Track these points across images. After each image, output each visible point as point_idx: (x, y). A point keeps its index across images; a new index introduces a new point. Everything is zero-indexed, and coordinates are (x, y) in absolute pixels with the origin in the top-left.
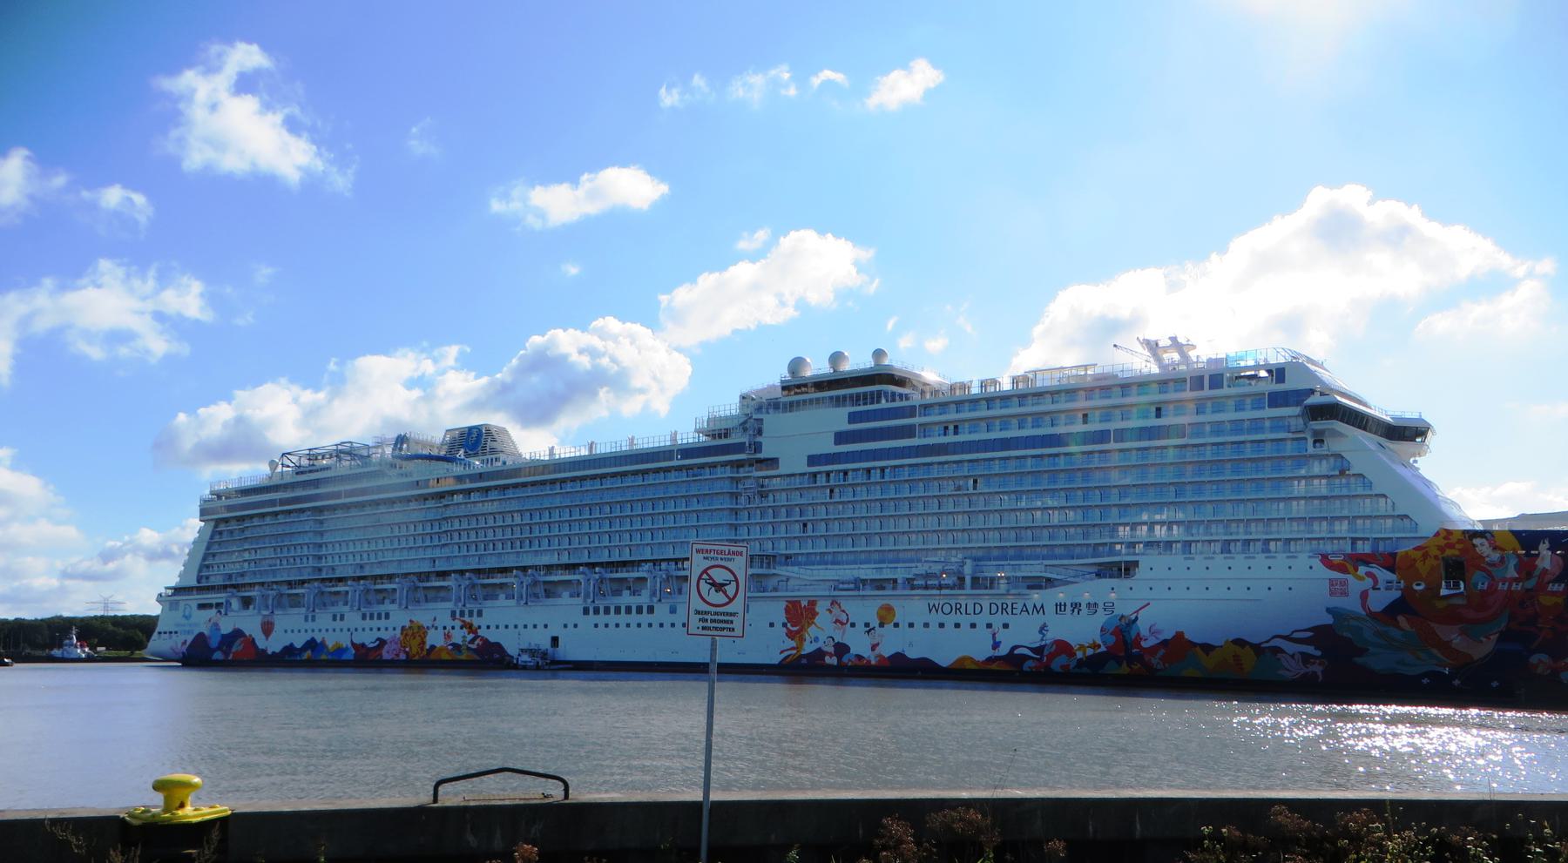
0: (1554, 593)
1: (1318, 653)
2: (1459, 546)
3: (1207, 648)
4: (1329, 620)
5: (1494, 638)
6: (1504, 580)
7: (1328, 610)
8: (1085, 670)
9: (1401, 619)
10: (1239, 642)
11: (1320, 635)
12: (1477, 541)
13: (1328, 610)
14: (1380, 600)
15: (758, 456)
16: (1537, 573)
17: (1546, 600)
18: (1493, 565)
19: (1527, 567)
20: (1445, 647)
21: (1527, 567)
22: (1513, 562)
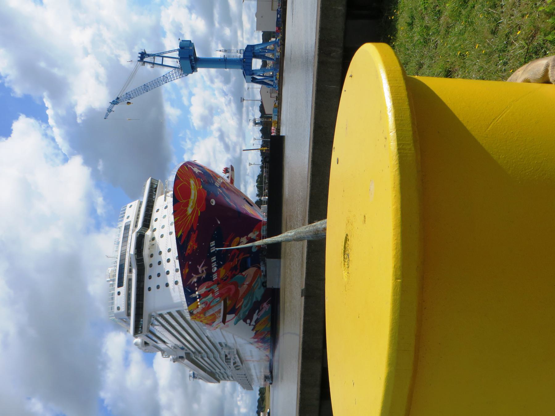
0: (218, 275)
1: (257, 311)
2: (198, 315)
3: (257, 332)
4: (241, 321)
5: (244, 273)
6: (213, 296)
7: (235, 324)
8: (269, 341)
9: (237, 308)
10: (253, 330)
11: (247, 318)
12: (195, 312)
13: (236, 323)
14: (229, 317)
15: (184, 356)
16: (209, 289)
17: (223, 271)
18: (206, 304)
19: (206, 295)
20: (249, 285)
21: (206, 295)
22: (204, 300)
